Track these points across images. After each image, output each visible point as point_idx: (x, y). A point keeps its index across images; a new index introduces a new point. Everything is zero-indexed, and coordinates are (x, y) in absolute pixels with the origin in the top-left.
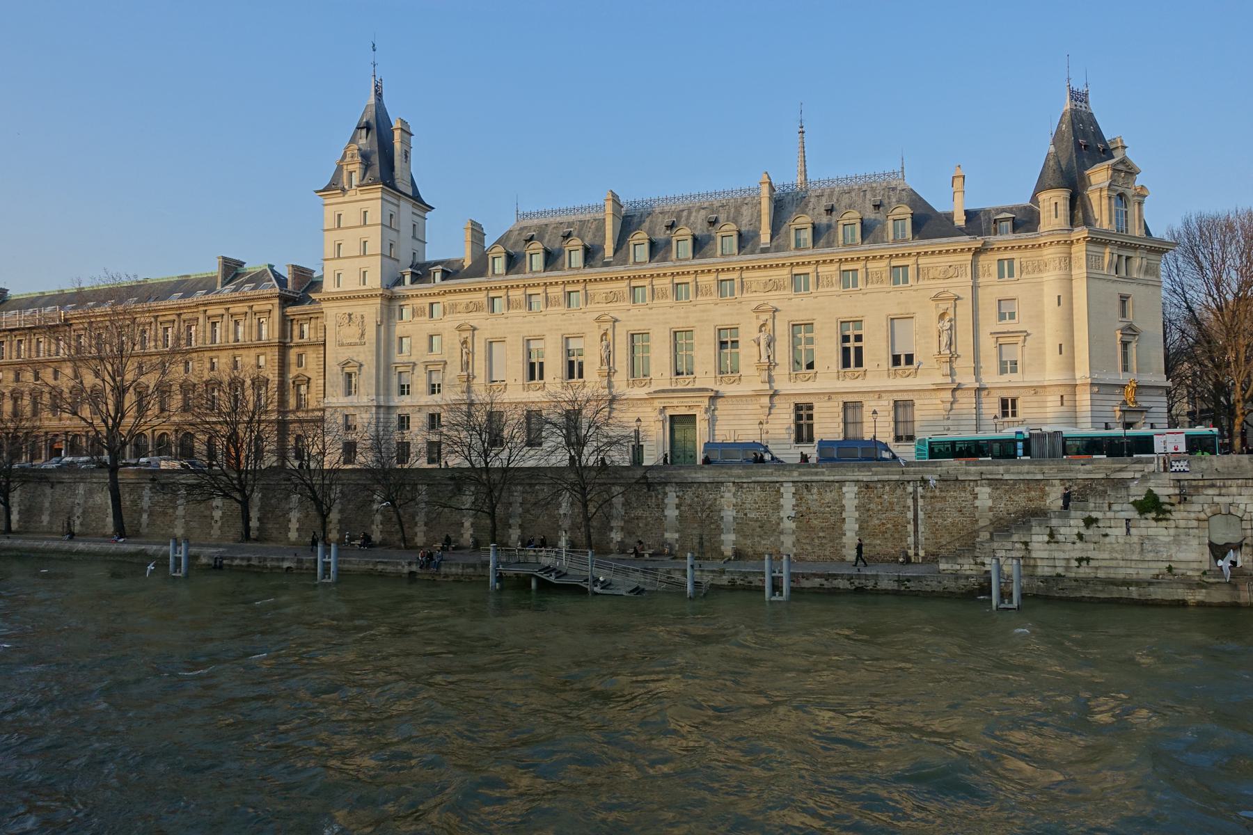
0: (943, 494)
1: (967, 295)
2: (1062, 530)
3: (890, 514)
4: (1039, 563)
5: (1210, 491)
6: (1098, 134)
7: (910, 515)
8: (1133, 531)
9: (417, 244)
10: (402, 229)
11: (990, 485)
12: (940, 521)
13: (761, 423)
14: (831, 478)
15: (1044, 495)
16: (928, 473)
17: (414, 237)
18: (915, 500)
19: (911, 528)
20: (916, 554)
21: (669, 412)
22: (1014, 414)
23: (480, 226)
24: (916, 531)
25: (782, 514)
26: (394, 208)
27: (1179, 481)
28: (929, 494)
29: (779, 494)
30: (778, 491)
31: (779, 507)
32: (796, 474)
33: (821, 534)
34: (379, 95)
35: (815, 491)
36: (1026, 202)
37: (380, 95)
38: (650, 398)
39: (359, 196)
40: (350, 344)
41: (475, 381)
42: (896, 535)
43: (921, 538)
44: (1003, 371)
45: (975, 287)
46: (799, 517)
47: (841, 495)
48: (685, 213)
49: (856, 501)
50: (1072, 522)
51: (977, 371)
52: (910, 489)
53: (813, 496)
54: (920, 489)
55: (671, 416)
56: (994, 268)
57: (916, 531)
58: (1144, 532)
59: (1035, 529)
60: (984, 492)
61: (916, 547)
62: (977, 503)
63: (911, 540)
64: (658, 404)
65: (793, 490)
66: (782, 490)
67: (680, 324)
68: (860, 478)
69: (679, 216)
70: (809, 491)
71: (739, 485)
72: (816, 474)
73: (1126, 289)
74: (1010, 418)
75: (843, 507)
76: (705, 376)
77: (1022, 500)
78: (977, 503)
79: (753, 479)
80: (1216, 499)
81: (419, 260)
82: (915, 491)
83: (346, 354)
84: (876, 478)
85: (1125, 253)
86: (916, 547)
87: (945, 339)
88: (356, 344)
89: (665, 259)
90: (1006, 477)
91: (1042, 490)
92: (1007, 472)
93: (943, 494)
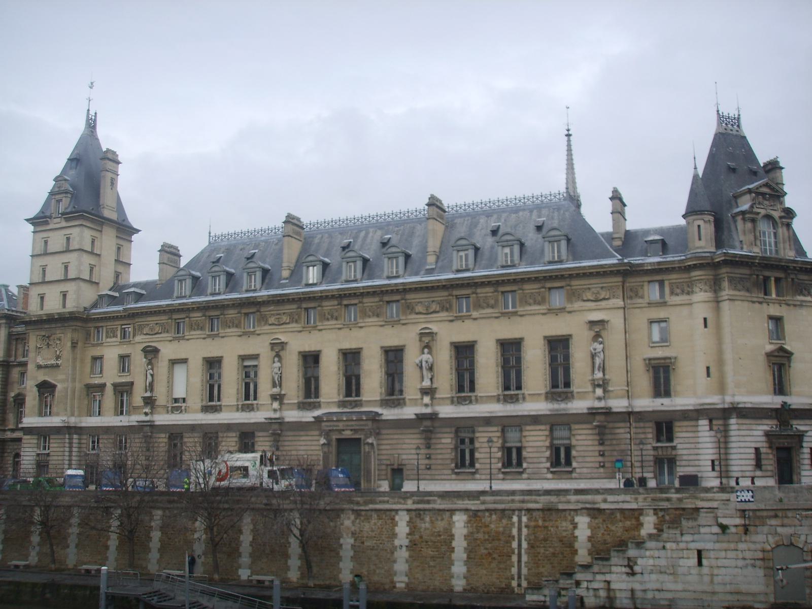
0: (547, 524)
2: (639, 561)
3: (496, 543)
4: (618, 594)
5: (773, 522)
6: (750, 155)
7: (515, 545)
8: (704, 562)
9: (120, 269)
10: (104, 253)
11: (589, 515)
12: (542, 551)
13: (418, 448)
14: (442, 507)
15: (640, 525)
16: (531, 502)
17: (117, 261)
18: (520, 530)
19: (515, 558)
20: (519, 585)
21: (334, 437)
23: (176, 248)
24: (519, 561)
25: (397, 542)
27: (744, 511)
28: (533, 524)
29: (395, 524)
30: (393, 519)
31: (394, 535)
32: (410, 502)
33: (432, 564)
34: (91, 125)
35: (428, 519)
37: (94, 127)
39: (64, 224)
40: (46, 367)
41: (157, 403)
42: (502, 566)
43: (524, 571)
46: (413, 546)
47: (451, 524)
48: (363, 234)
49: (465, 531)
50: (648, 553)
52: (515, 519)
53: (425, 525)
54: (524, 519)
55: (337, 439)
57: (519, 561)
58: (714, 562)
59: (614, 560)
60: (583, 521)
61: (519, 577)
62: (577, 533)
63: (514, 570)
65: (407, 518)
66: (397, 518)
68: (469, 507)
69: (356, 238)
70: (422, 519)
71: (357, 513)
72: (428, 502)
73: (774, 310)
75: (452, 537)
77: (618, 529)
78: (577, 533)
79: (371, 506)
80: (779, 530)
81: (121, 282)
82: (520, 521)
83: (42, 377)
84: (483, 507)
86: (519, 577)
88: (52, 366)
89: (334, 281)
90: (603, 506)
91: (638, 519)
92: (605, 501)
93: (547, 524)
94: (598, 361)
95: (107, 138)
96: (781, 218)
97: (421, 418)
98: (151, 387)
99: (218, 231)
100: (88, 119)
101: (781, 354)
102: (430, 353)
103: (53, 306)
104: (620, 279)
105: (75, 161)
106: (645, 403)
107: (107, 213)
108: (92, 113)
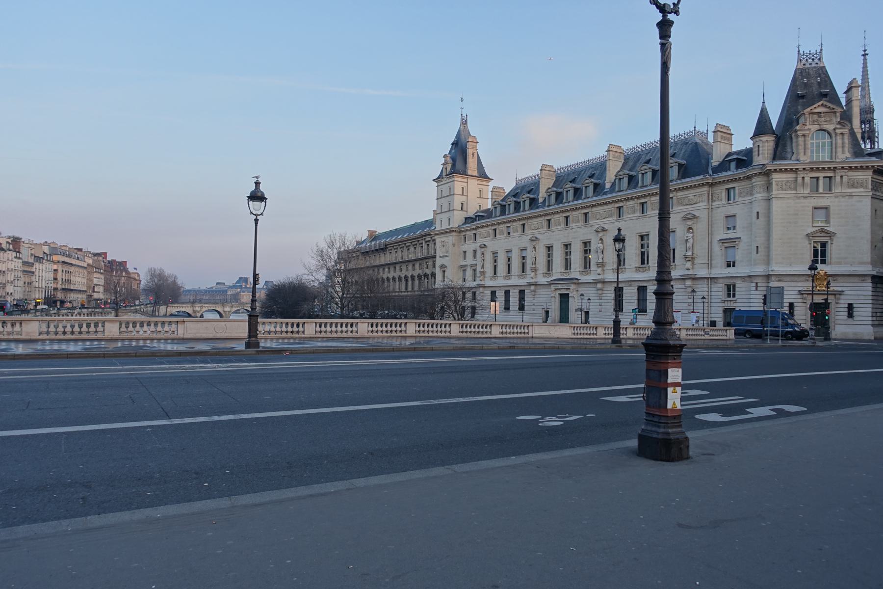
1: (703, 214)
9: (481, 201)
22: (734, 296)
26: (465, 184)
36: (750, 144)
38: (549, 284)
44: (729, 265)
45: (711, 210)
51: (710, 265)
56: (724, 195)
64: (553, 287)
67: (566, 241)
74: (731, 299)
76: (576, 271)
85: (821, 175)
87: (689, 244)
94: (689, 244)
95: (473, 129)
96: (835, 129)
97: (595, 282)
98: (483, 266)
99: (519, 178)
100: (462, 120)
101: (823, 234)
102: (602, 243)
103: (445, 226)
104: (706, 189)
105: (455, 144)
106: (720, 271)
107: (470, 173)
108: (464, 115)
